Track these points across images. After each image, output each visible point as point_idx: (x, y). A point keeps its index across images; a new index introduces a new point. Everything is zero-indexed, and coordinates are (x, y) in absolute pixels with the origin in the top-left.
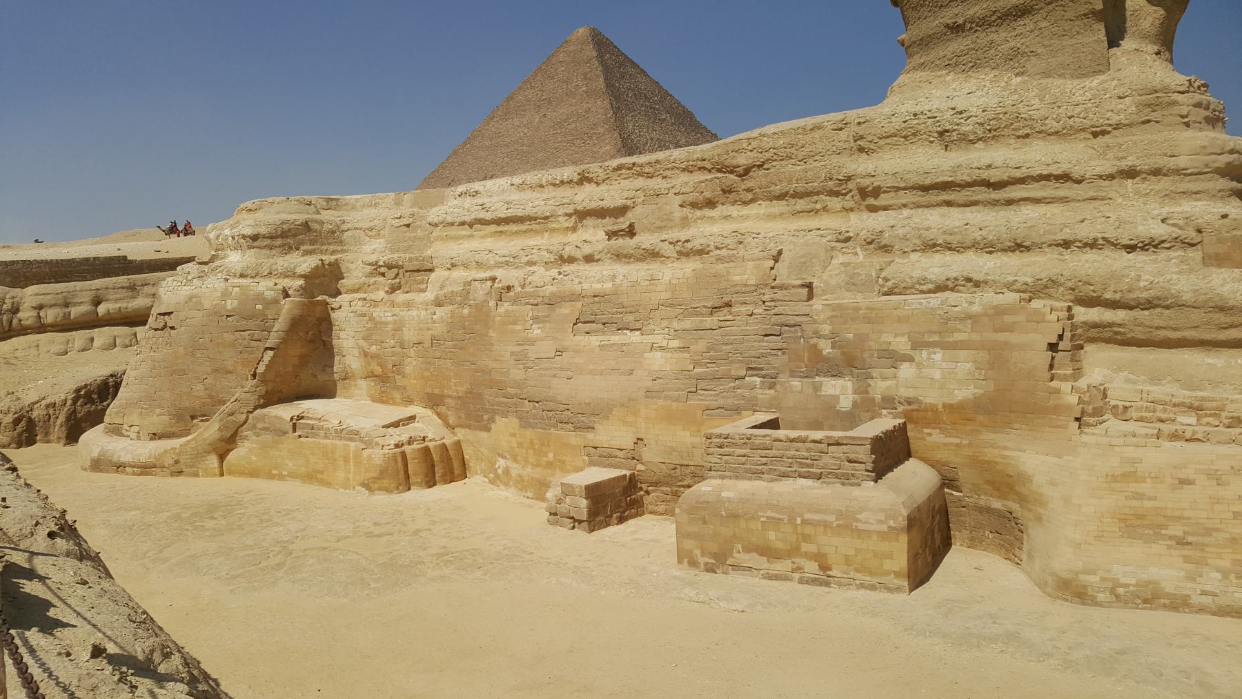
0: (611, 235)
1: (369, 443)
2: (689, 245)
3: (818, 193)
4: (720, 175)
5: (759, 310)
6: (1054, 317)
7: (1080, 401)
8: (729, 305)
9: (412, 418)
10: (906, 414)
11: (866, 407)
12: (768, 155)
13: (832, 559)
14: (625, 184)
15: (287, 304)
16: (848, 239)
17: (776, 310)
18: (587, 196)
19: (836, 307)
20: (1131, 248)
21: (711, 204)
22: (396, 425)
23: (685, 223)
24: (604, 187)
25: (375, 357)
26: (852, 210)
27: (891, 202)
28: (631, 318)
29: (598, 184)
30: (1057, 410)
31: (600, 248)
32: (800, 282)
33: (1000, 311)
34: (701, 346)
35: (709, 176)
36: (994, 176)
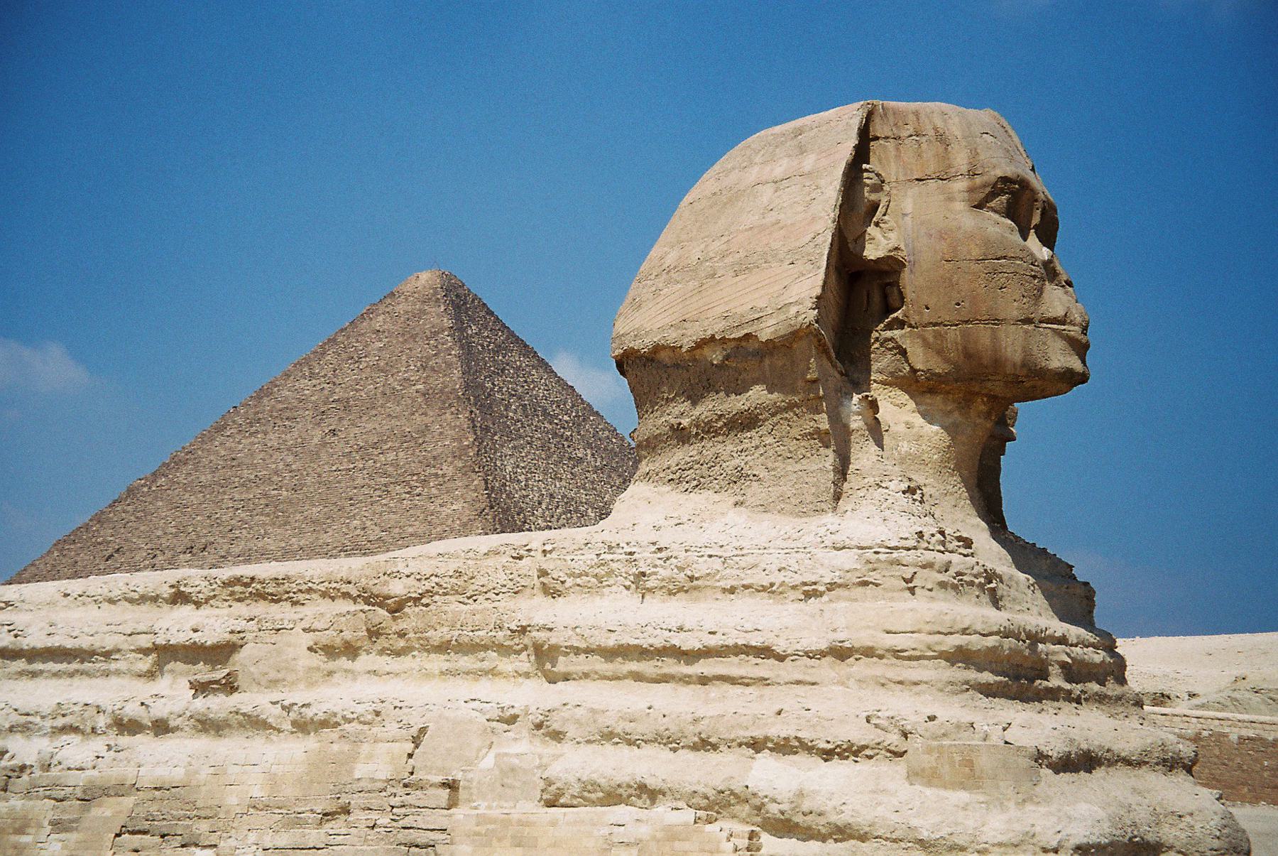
0: (201, 688)
2: (309, 713)
3: (486, 648)
4: (367, 608)
5: (384, 820)
6: (730, 846)
12: (428, 585)
14: (242, 609)
16: (512, 720)
17: (407, 822)
18: (178, 625)
19: (482, 819)
20: (828, 755)
21: (351, 650)
24: (205, 611)
26: (527, 675)
27: (571, 669)
28: (204, 826)
29: (198, 604)
31: (178, 708)
32: (440, 779)
33: (671, 834)
35: (352, 608)
36: (689, 642)
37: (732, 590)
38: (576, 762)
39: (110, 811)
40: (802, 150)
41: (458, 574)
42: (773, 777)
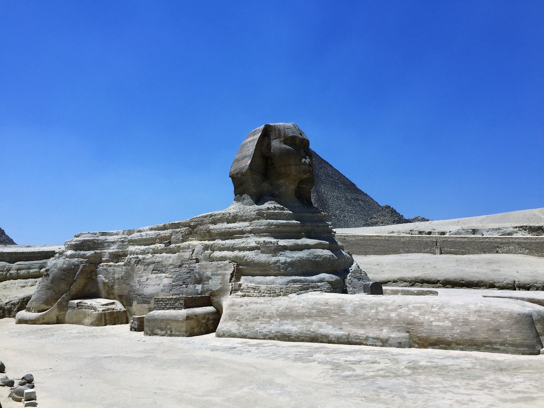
1: (95, 309)
7: (232, 288)
8: (183, 264)
9: (113, 303)
10: (210, 294)
11: (202, 292)
13: (173, 329)
15: (81, 266)
22: (107, 305)
23: (183, 241)
25: (107, 283)
28: (164, 268)
30: (228, 290)
33: (225, 265)
34: (174, 276)
36: (231, 230)
37: (239, 221)
38: (217, 254)
39: (151, 267)
40: (254, 135)
41: (201, 221)
42: (241, 254)
